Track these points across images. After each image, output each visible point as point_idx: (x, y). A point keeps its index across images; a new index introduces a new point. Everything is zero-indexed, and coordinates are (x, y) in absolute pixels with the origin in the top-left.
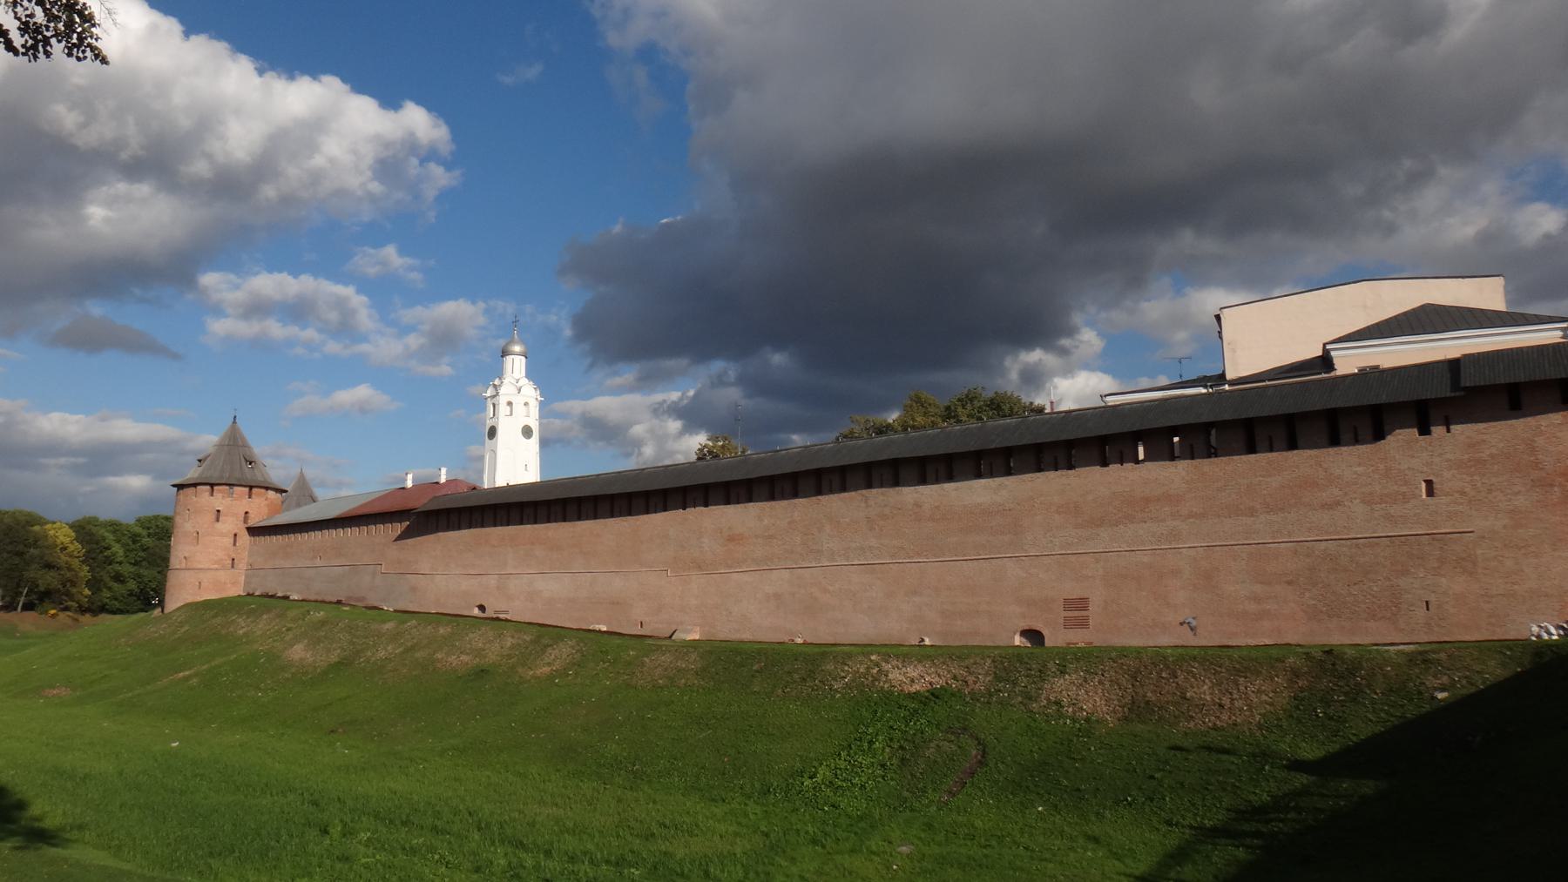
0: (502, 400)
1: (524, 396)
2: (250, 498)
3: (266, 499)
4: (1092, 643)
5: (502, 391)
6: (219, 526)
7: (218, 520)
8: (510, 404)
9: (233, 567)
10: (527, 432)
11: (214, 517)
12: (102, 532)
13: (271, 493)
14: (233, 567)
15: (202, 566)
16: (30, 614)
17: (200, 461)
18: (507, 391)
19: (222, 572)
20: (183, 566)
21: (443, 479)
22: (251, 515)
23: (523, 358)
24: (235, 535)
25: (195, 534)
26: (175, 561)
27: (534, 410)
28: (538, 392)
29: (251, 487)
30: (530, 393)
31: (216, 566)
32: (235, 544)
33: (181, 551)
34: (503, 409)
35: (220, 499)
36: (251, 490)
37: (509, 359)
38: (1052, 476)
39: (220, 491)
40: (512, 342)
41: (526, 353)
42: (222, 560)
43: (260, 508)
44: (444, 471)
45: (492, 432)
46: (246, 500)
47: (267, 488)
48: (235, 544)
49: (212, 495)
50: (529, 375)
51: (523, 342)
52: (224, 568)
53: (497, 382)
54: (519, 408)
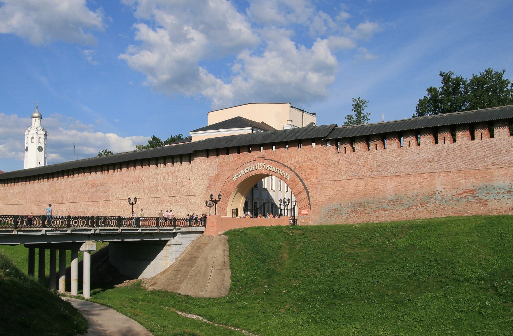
37: (33, 119)
40: (34, 112)
45: (27, 149)
53: (29, 129)
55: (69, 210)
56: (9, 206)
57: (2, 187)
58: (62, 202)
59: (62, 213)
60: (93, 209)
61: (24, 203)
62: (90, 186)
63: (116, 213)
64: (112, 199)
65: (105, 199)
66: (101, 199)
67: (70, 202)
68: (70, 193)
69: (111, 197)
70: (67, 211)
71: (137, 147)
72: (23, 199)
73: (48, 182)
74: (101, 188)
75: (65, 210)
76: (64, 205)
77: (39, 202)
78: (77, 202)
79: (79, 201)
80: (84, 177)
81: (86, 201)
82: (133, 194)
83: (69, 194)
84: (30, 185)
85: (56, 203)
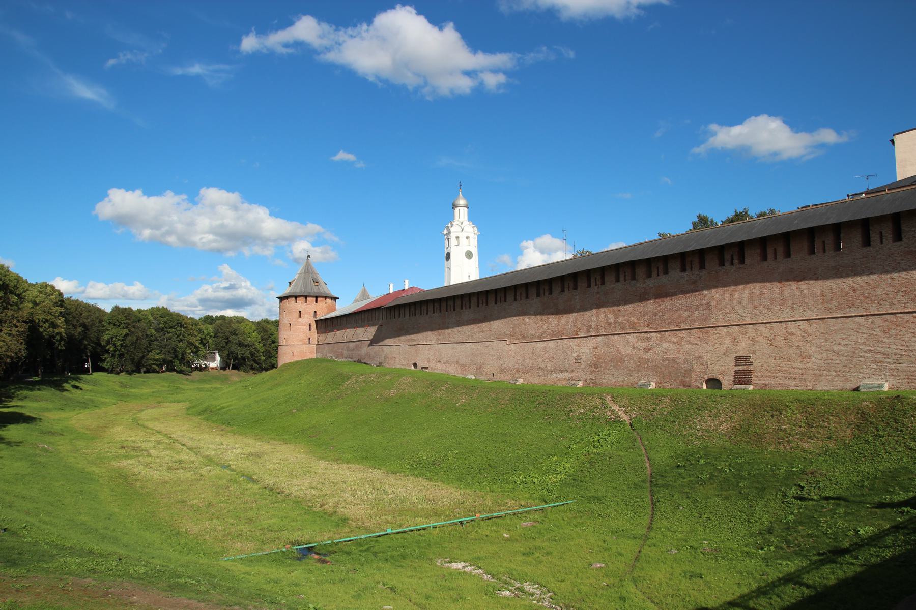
0: (453, 237)
1: (465, 232)
2: (316, 302)
3: (326, 304)
4: (253, 374)
5: (452, 230)
6: (300, 319)
7: (300, 317)
8: (457, 238)
9: (310, 343)
10: (469, 255)
12: (269, 326)
13: (328, 301)
14: (310, 343)
15: (292, 343)
16: (236, 371)
18: (455, 230)
19: (304, 346)
20: (284, 343)
21: (406, 288)
22: (317, 313)
23: (466, 209)
24: (310, 325)
25: (289, 325)
26: (282, 341)
27: (474, 242)
28: (476, 229)
29: (316, 297)
30: (470, 230)
31: (301, 343)
32: (310, 330)
33: (284, 335)
34: (453, 241)
35: (300, 305)
36: (306, 299)
37: (457, 209)
39: (300, 300)
40: (457, 197)
41: (467, 205)
42: (304, 339)
43: (324, 310)
44: (407, 282)
45: (448, 257)
47: (326, 297)
48: (310, 330)
50: (469, 220)
51: (465, 197)
52: (304, 344)
55: (596, 350)
63: (738, 354)
64: (719, 325)
69: (716, 320)
70: (592, 353)
71: (659, 236)
73: (539, 298)
80: (633, 282)
84: (496, 306)
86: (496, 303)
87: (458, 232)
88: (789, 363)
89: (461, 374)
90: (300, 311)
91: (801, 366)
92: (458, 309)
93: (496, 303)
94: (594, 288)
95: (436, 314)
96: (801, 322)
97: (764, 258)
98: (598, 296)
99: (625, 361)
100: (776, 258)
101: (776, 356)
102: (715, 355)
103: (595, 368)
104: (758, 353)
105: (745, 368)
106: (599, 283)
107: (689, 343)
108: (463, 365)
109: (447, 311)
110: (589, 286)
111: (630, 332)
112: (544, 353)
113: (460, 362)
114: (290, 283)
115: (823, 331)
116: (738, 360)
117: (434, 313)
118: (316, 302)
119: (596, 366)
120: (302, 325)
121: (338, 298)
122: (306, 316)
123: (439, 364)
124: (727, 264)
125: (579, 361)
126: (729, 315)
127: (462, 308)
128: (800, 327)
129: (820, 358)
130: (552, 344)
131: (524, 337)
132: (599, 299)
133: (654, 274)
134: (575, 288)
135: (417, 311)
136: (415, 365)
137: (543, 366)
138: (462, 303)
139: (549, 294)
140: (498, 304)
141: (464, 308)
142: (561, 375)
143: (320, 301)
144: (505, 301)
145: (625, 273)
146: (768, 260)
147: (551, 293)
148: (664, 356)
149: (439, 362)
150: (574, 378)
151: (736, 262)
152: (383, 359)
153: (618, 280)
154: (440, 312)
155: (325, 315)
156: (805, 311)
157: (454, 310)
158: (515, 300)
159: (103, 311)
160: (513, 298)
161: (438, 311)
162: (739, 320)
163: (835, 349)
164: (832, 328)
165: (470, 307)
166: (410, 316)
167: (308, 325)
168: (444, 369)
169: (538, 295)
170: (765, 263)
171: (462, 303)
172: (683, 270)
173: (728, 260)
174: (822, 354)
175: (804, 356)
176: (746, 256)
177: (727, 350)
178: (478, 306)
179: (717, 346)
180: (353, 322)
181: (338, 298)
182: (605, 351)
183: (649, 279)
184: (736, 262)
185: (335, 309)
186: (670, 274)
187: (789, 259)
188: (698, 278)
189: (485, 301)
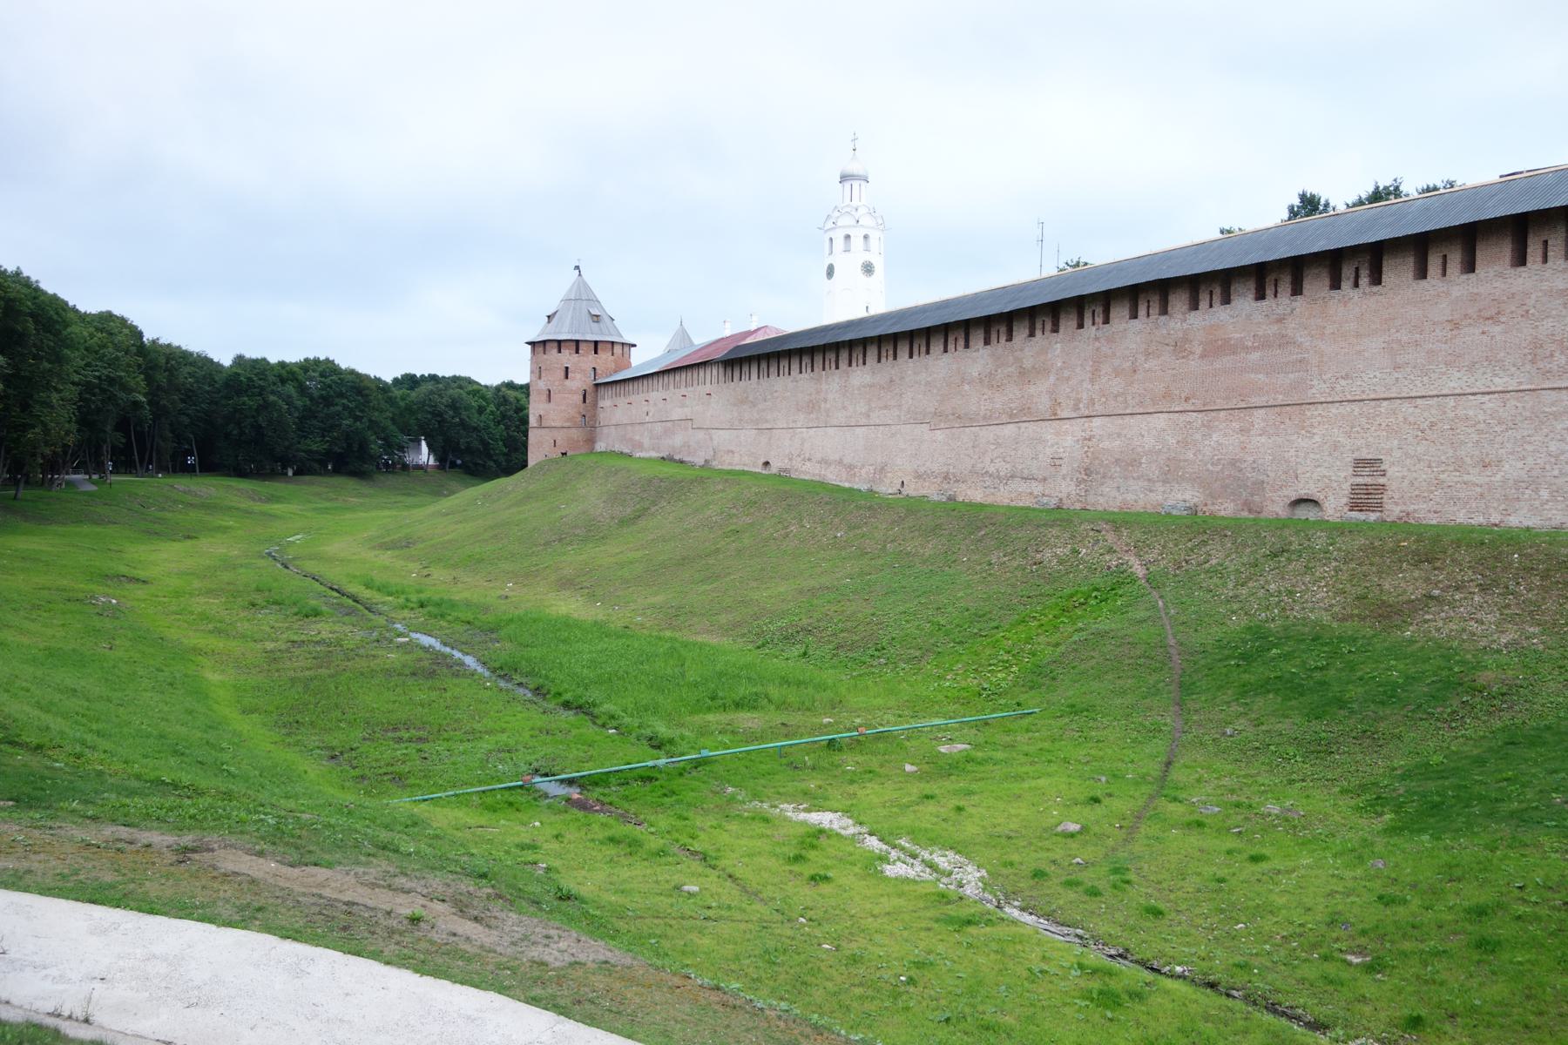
2: (596, 352)
6: (567, 382)
7: (567, 377)
8: (848, 237)
11: (563, 374)
15: (553, 424)
17: (549, 317)
19: (574, 430)
23: (863, 183)
32: (584, 401)
35: (567, 357)
38: (1321, 243)
39: (567, 348)
45: (830, 272)
46: (592, 355)
48: (584, 401)
49: (560, 352)
54: (857, 242)
55: (1090, 443)
56: (831, 431)
57: (804, 370)
58: (1055, 414)
59: (1057, 453)
60: (1215, 437)
61: (890, 422)
62: (1198, 350)
63: (1357, 455)
64: (1323, 400)
65: (1280, 399)
66: (1255, 401)
67: (1095, 413)
68: (1092, 381)
69: (1318, 390)
72: (886, 407)
73: (988, 347)
74: (1256, 356)
75: (1069, 441)
76: (1066, 426)
77: (951, 417)
78: (1128, 411)
79: (1141, 411)
80: (1163, 318)
81: (1177, 409)
82: (1458, 375)
83: (1086, 385)
85: (1024, 419)
86: (911, 357)
87: (849, 226)
88: (1458, 474)
89: (847, 480)
90: (567, 368)
91: (1481, 480)
92: (843, 364)
93: (911, 357)
94: (1090, 330)
95: (804, 375)
96: (1487, 397)
97: (1422, 273)
98: (1097, 344)
99: (1141, 463)
100: (1444, 274)
101: (1433, 459)
102: (1312, 456)
103: (1086, 475)
104: (1396, 454)
105: (1369, 480)
106: (1099, 320)
107: (1263, 433)
108: (850, 467)
109: (824, 369)
110: (1081, 326)
111: (1152, 410)
112: (993, 447)
113: (845, 461)
114: (549, 317)
115: (1528, 414)
116: (1360, 464)
117: (801, 372)
118: (596, 352)
119: (1088, 472)
120: (571, 392)
121: (634, 346)
122: (578, 376)
123: (808, 463)
124: (1346, 285)
125: (1058, 462)
126: (1343, 382)
127: (850, 365)
128: (1484, 407)
129: (1520, 465)
130: (1010, 430)
131: (959, 417)
132: (1097, 349)
133: (1204, 304)
134: (1055, 330)
135: (771, 370)
136: (767, 464)
137: (992, 469)
138: (850, 355)
139: (1007, 341)
140: (915, 357)
141: (854, 364)
142: (1023, 487)
143: (602, 350)
144: (928, 352)
145: (1149, 301)
146: (1428, 277)
147: (1010, 339)
148: (1216, 455)
149: (809, 460)
150: (1047, 492)
151: (1364, 281)
152: (712, 453)
153: (1134, 316)
154: (812, 370)
155: (611, 375)
156: (1496, 375)
157: (837, 368)
158: (946, 351)
159: (218, 365)
160: (942, 347)
161: (809, 370)
162: (1363, 392)
163: (1550, 449)
164: (1547, 410)
165: (864, 363)
166: (759, 378)
167: (582, 393)
168: (817, 472)
169: (987, 342)
170: (1423, 283)
171: (850, 355)
172: (1261, 296)
173: (1348, 279)
174: (1524, 458)
175: (1487, 461)
176: (1384, 269)
177: (1336, 446)
178: (879, 361)
179: (1317, 438)
180: (661, 388)
181: (634, 346)
182: (1106, 444)
183: (1193, 313)
184: (1364, 281)
185: (628, 365)
186: (1233, 304)
187: (1471, 276)
188: (1289, 310)
189: (891, 352)
